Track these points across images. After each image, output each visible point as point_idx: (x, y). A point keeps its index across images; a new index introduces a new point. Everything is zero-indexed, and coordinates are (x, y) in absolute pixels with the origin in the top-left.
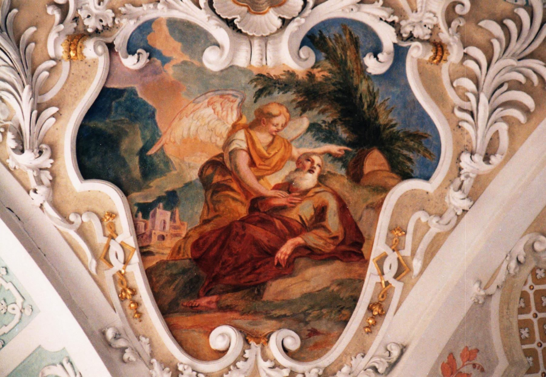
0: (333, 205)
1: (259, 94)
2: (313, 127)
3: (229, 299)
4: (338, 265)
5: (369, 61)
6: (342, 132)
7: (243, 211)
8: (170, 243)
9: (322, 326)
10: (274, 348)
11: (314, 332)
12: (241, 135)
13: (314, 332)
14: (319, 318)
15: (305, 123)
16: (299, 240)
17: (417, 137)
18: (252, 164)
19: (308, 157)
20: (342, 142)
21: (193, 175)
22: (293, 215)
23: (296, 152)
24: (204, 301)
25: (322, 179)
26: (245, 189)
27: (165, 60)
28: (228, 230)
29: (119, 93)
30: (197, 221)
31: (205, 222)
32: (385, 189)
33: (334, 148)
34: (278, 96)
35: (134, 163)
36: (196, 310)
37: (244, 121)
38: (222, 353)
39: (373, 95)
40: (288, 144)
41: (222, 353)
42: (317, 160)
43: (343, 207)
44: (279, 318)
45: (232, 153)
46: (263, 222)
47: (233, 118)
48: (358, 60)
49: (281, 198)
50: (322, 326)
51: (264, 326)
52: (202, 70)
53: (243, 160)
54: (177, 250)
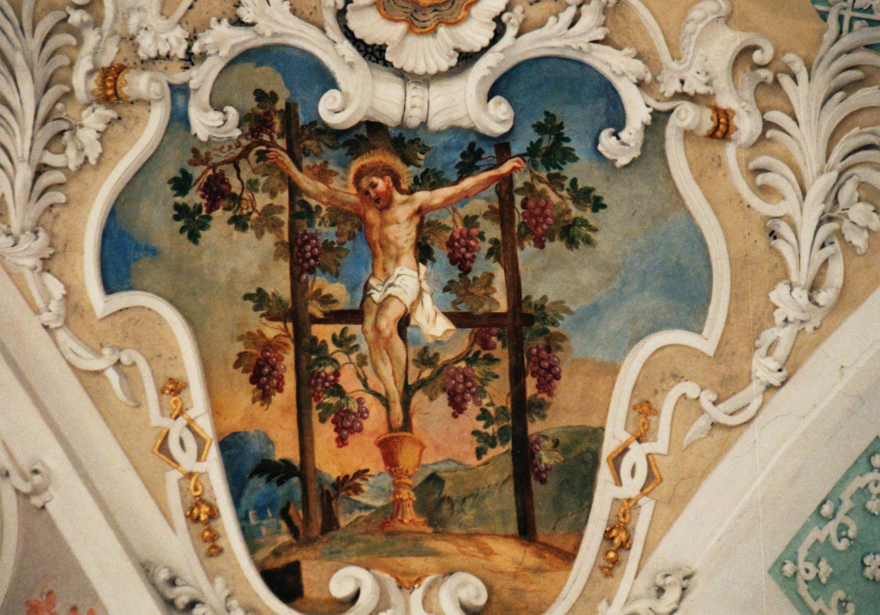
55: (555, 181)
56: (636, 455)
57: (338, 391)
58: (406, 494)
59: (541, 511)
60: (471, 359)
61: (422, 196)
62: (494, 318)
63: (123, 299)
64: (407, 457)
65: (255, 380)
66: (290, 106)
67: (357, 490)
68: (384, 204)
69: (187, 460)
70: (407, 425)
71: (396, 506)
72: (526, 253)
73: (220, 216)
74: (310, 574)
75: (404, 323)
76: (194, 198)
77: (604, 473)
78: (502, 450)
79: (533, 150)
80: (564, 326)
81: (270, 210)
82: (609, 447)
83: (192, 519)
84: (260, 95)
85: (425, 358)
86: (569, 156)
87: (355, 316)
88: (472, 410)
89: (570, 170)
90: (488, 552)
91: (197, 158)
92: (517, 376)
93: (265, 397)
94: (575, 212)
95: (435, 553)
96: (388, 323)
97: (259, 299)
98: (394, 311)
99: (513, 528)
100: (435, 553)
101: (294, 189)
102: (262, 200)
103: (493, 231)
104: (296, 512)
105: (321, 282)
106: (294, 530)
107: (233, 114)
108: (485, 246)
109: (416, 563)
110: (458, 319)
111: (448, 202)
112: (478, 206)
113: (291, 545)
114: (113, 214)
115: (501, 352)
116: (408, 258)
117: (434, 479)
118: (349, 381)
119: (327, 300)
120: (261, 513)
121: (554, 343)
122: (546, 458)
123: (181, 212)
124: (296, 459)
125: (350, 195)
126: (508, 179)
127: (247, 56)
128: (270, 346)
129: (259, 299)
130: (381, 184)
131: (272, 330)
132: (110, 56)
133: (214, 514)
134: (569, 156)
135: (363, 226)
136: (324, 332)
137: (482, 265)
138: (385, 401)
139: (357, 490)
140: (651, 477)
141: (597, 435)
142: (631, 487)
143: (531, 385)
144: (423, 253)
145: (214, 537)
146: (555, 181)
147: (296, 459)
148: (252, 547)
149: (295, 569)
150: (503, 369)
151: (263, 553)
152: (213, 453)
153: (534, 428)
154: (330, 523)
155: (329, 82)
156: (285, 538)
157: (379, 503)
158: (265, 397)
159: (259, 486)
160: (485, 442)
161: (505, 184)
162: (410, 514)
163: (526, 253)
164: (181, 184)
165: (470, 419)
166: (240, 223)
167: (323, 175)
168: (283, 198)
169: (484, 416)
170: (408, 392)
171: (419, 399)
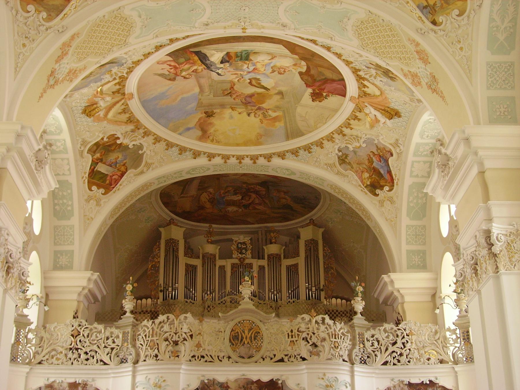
9: (53, 14)
10: (41, 16)
11: (50, 15)
13: (50, 15)
14: (53, 12)
38: (29, 12)
41: (29, 12)
44: (45, 8)
51: (41, 9)
67: (436, 5)
69: (414, 11)
71: (442, 4)
74: (436, 20)
83: (419, 20)
90: (456, 4)
95: (450, 8)
100: (450, 8)
104: (431, 12)
106: (432, 14)
109: (448, 11)
113: (432, 17)
120: (427, 14)
124: (427, 4)
133: (421, 18)
139: (436, 5)
145: (422, 20)
147: (427, 4)
148: (428, 19)
151: (430, 20)
152: (417, 9)
154: (435, 11)
156: (432, 16)
157: (440, 5)
159: (424, 10)
162: (444, 4)
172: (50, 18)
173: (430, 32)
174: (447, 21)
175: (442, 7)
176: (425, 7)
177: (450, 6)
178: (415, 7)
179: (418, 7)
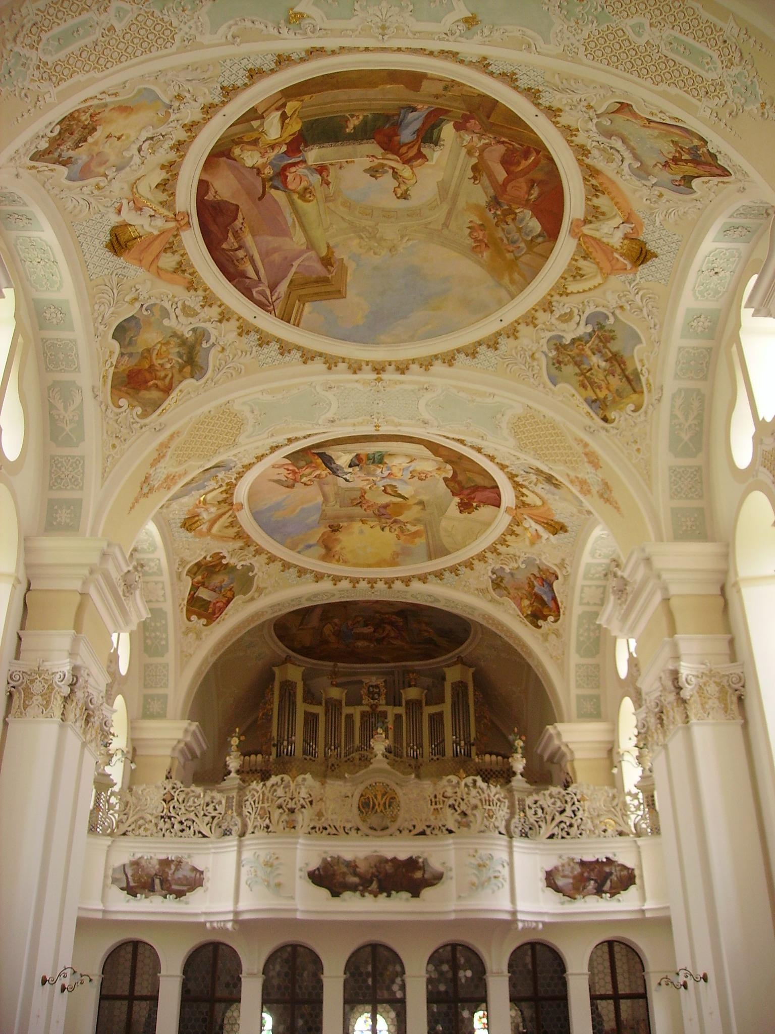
0: (170, 376)
1: (171, 336)
2: (178, 352)
3: (131, 391)
4: (161, 393)
5: (204, 342)
6: (185, 358)
7: (147, 366)
8: (124, 367)
9: (149, 410)
10: (134, 412)
12: (159, 345)
13: (146, 410)
15: (177, 350)
16: (156, 381)
17: (202, 368)
18: (157, 354)
19: (172, 359)
20: (182, 360)
21: (140, 350)
22: (158, 374)
23: (170, 357)
24: (123, 388)
25: (172, 367)
26: (151, 360)
27: (153, 315)
28: (140, 371)
29: (136, 318)
30: (134, 364)
31: (136, 365)
32: (185, 378)
33: (180, 361)
34: (175, 339)
35: (128, 340)
36: (120, 390)
37: (163, 342)
38: (120, 407)
39: (199, 351)
40: (169, 353)
41: (120, 407)
42: (174, 361)
43: (172, 378)
44: (139, 402)
45: (154, 349)
46: (150, 372)
47: (160, 340)
48: (201, 340)
49: (158, 368)
50: (149, 410)
51: (136, 403)
52: (162, 322)
53: (156, 352)
54: (124, 370)
55: (605, 331)
56: (644, 369)
57: (596, 383)
58: (615, 395)
59: (635, 386)
60: (611, 367)
61: (588, 345)
62: (611, 358)
63: (558, 386)
64: (611, 388)
65: (584, 387)
66: (560, 344)
68: (583, 350)
70: (609, 383)
71: (614, 398)
72: (608, 345)
73: (562, 365)
74: (608, 416)
75: (598, 366)
76: (557, 365)
77: (641, 376)
78: (624, 380)
79: (598, 329)
80: (622, 353)
81: (568, 361)
82: (639, 370)
84: (555, 344)
85: (605, 370)
86: (604, 326)
87: (591, 369)
88: (616, 375)
89: (606, 328)
91: (553, 359)
92: (620, 365)
93: (586, 389)
94: (612, 334)
96: (596, 367)
97: (576, 374)
98: (596, 365)
99: (632, 392)
101: (569, 355)
102: (566, 359)
103: (601, 345)
105: (583, 367)
107: (553, 351)
108: (602, 348)
109: (622, 406)
110: (606, 361)
111: (592, 344)
112: (597, 342)
114: (548, 374)
115: (615, 363)
116: (592, 355)
117: (617, 390)
118: (596, 380)
119: (585, 369)
121: (622, 357)
122: (631, 377)
123: (557, 368)
124: (595, 397)
125: (577, 351)
126: (598, 335)
127: (548, 341)
128: (582, 381)
129: (576, 374)
130: (581, 347)
131: (581, 378)
132: (531, 353)
134: (604, 326)
135: (583, 355)
136: (588, 374)
137: (604, 351)
138: (602, 380)
140: (649, 372)
141: (636, 369)
142: (646, 374)
143: (622, 365)
144: (594, 354)
146: (605, 331)
148: (598, 415)
149: (605, 416)
150: (617, 366)
153: (627, 373)
154: (607, 406)
155: (562, 337)
158: (586, 389)
159: (594, 405)
160: (621, 379)
161: (598, 337)
162: (617, 398)
163: (608, 345)
164: (554, 364)
165: (617, 377)
166: (566, 365)
167: (571, 351)
168: (569, 357)
169: (619, 375)
170: (605, 377)
171: (608, 378)
172: (145, 415)
173: (601, 430)
174: (620, 417)
175: (614, 401)
176: (594, 401)
177: (624, 400)
178: (582, 400)
179: (586, 400)
